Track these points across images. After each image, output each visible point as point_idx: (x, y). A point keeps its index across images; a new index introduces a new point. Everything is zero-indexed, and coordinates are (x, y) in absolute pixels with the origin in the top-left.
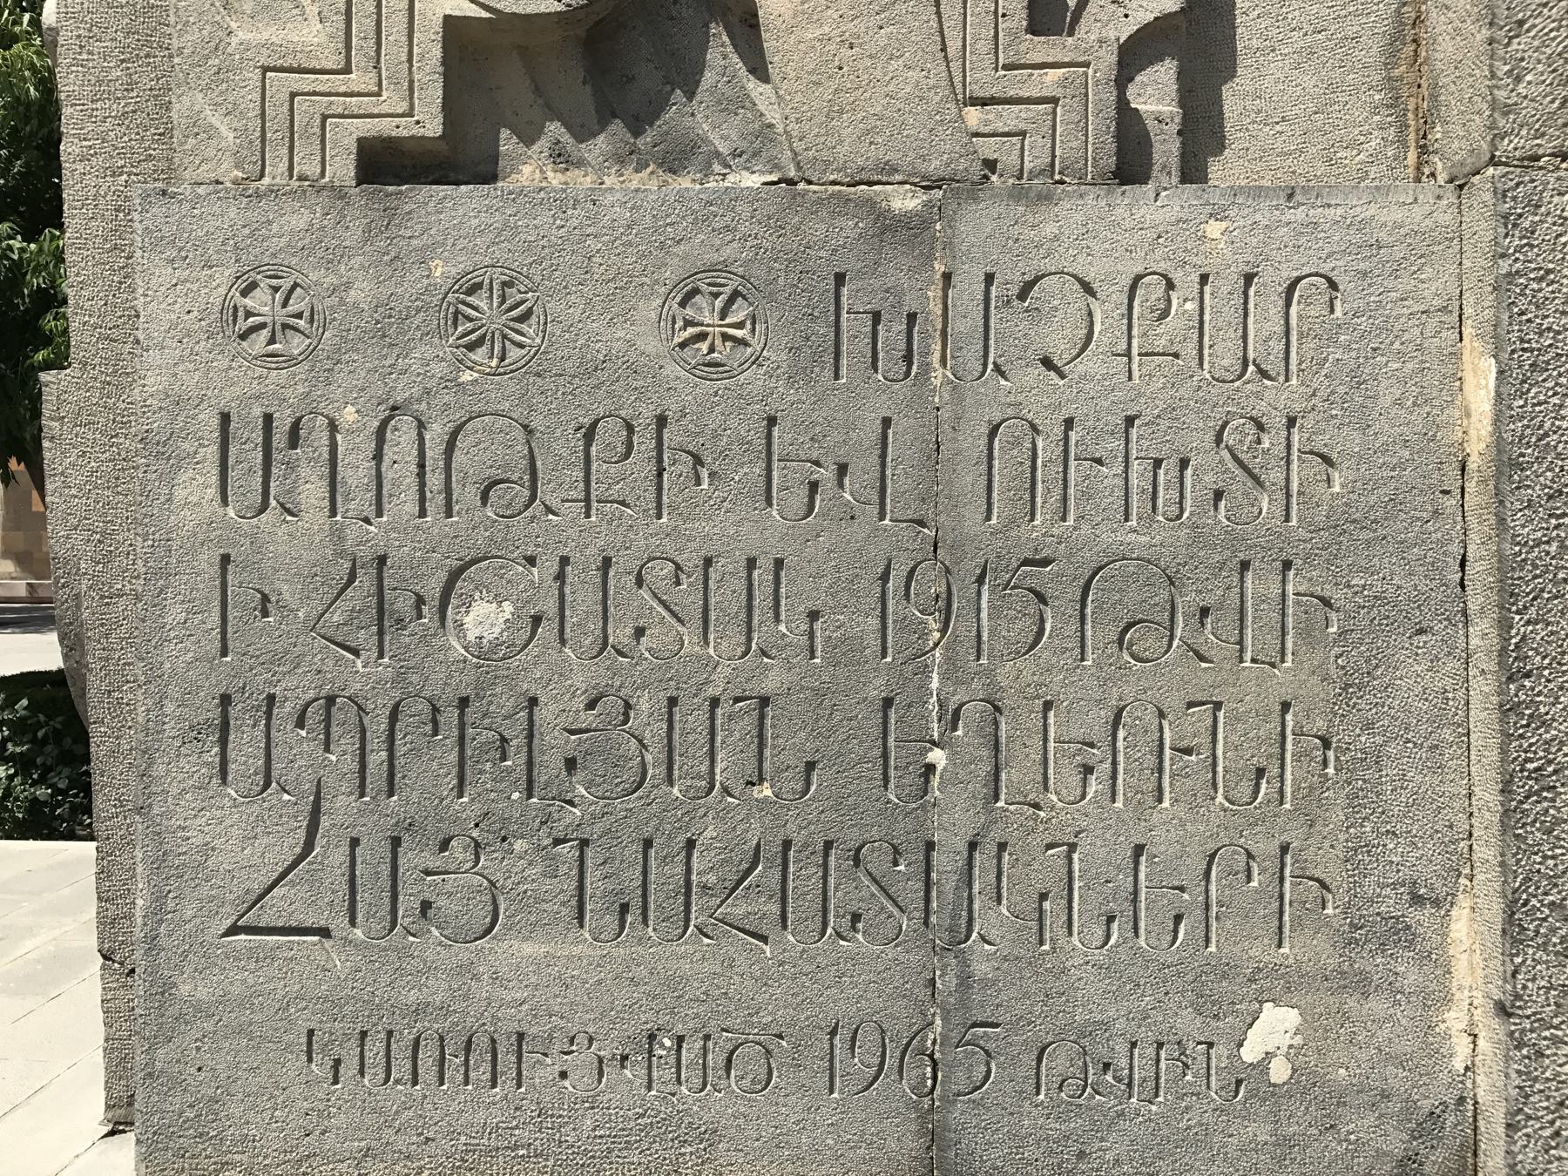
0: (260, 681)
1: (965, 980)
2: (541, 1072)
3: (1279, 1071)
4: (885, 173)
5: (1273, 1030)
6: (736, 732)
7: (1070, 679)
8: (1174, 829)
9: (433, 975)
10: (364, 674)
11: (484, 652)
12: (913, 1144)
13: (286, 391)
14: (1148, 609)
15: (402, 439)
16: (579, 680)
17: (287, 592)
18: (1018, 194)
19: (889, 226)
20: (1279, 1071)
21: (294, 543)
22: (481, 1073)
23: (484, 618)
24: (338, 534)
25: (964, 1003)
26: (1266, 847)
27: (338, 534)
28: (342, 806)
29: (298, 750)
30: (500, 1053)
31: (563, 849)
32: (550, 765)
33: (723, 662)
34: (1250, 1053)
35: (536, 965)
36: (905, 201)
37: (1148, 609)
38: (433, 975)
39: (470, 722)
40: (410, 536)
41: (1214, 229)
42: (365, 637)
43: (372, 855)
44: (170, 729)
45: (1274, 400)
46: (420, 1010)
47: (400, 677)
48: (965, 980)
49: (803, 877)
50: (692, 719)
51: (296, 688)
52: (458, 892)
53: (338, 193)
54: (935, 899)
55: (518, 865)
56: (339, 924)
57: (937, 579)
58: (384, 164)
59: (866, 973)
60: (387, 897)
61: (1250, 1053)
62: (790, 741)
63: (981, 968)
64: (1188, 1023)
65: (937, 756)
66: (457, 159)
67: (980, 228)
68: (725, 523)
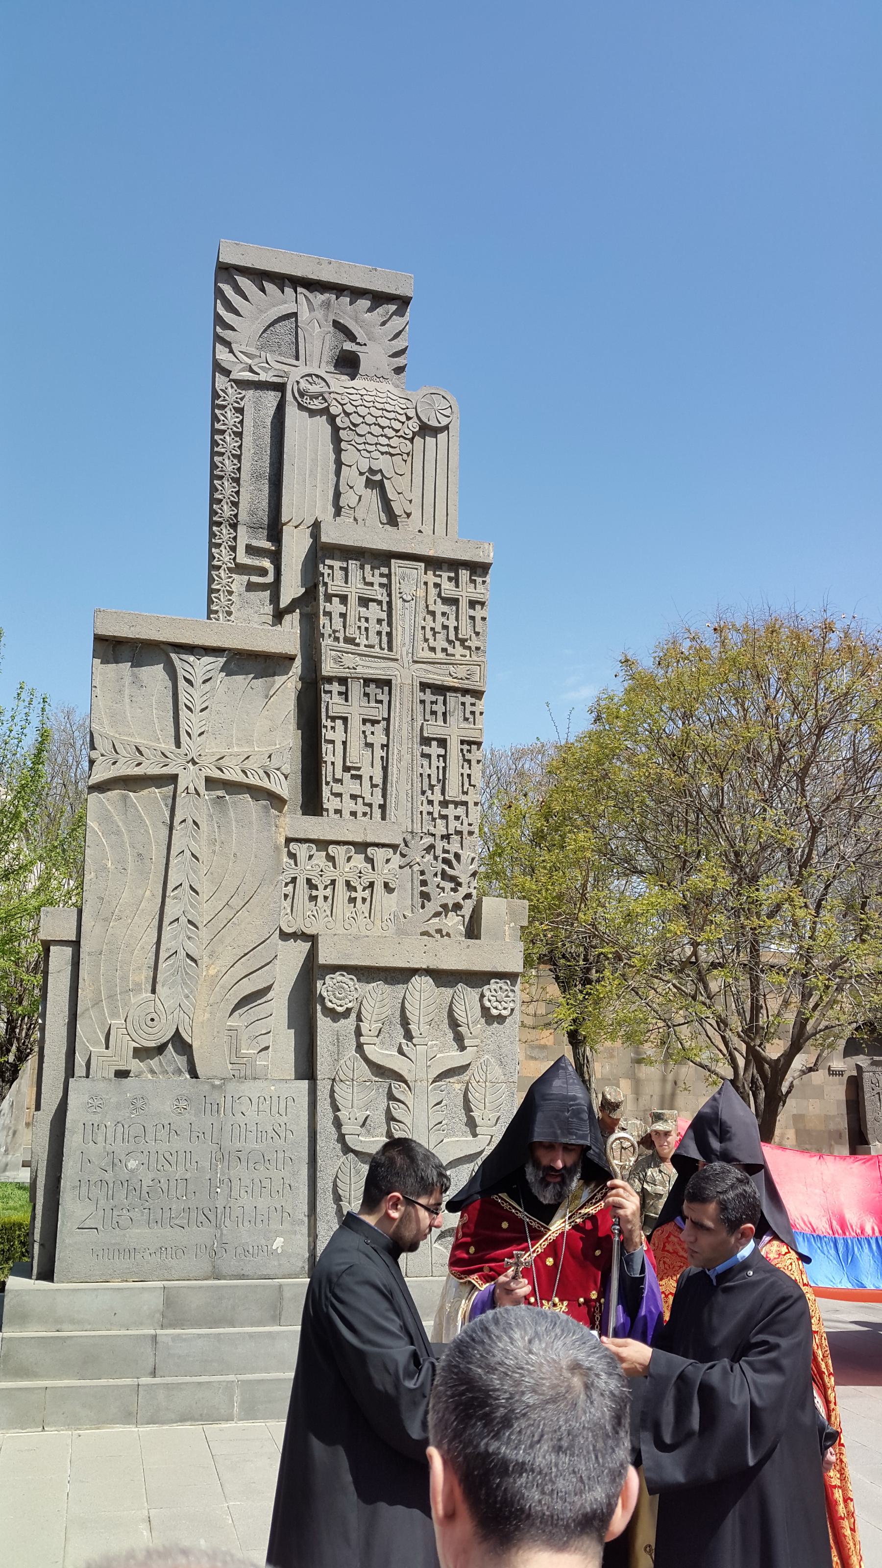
0: (86, 1178)
1: (222, 1234)
2: (139, 1256)
3: (279, 1251)
4: (215, 1077)
5: (279, 1242)
6: (182, 1184)
8: (262, 1203)
10: (109, 1176)
11: (132, 1171)
12: (210, 1268)
13: (96, 1119)
15: (120, 1129)
16: (151, 1175)
17: (93, 1159)
18: (238, 1081)
19: (214, 1086)
20: (279, 1251)
22: (127, 1256)
24: (105, 1147)
25: (221, 1239)
26: (279, 1207)
27: (105, 1147)
28: (102, 1202)
29: (95, 1192)
31: (146, 1211)
32: (144, 1193)
33: (180, 1173)
34: (274, 1247)
35: (139, 1235)
36: (217, 1082)
39: (128, 1184)
40: (120, 1147)
41: (273, 1088)
42: (109, 1169)
43: (108, 1212)
44: (68, 1187)
45: (285, 1119)
46: (115, 1244)
47: (115, 1176)
48: (222, 1234)
49: (193, 1214)
50: (173, 1183)
51: (94, 1178)
53: (110, 1080)
55: (136, 1214)
56: (100, 1227)
57: (221, 1155)
59: (204, 1234)
61: (274, 1247)
62: (191, 1187)
63: (225, 1232)
64: (263, 1242)
65: (218, 1190)
67: (231, 1087)
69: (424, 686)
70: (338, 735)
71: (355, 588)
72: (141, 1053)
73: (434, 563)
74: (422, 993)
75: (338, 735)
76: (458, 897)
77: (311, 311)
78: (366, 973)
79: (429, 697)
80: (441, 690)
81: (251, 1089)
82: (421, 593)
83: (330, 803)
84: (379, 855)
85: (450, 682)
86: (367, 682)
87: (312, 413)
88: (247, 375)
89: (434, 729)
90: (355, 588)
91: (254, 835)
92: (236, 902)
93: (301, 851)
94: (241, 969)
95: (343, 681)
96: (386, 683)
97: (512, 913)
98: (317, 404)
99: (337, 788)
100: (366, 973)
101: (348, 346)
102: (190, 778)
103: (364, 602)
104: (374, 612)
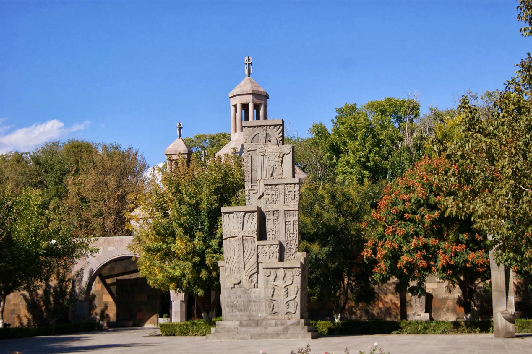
5: (260, 315)
7: (253, 304)
9: (234, 314)
14: (256, 301)
21: (229, 300)
23: (235, 302)
30: (236, 316)
35: (237, 313)
37: (256, 301)
38: (234, 314)
39: (235, 306)
52: (234, 310)
54: (249, 311)
59: (247, 313)
60: (232, 311)
66: (234, 288)
67: (250, 290)
68: (242, 299)
70: (269, 223)
71: (270, 193)
72: (234, 284)
75: (269, 223)
76: (293, 252)
79: (286, 212)
81: (254, 290)
82: (284, 191)
85: (290, 209)
88: (250, 149)
89: (287, 219)
90: (270, 193)
92: (249, 258)
94: (250, 269)
97: (303, 255)
98: (262, 154)
99: (269, 233)
104: (274, 196)
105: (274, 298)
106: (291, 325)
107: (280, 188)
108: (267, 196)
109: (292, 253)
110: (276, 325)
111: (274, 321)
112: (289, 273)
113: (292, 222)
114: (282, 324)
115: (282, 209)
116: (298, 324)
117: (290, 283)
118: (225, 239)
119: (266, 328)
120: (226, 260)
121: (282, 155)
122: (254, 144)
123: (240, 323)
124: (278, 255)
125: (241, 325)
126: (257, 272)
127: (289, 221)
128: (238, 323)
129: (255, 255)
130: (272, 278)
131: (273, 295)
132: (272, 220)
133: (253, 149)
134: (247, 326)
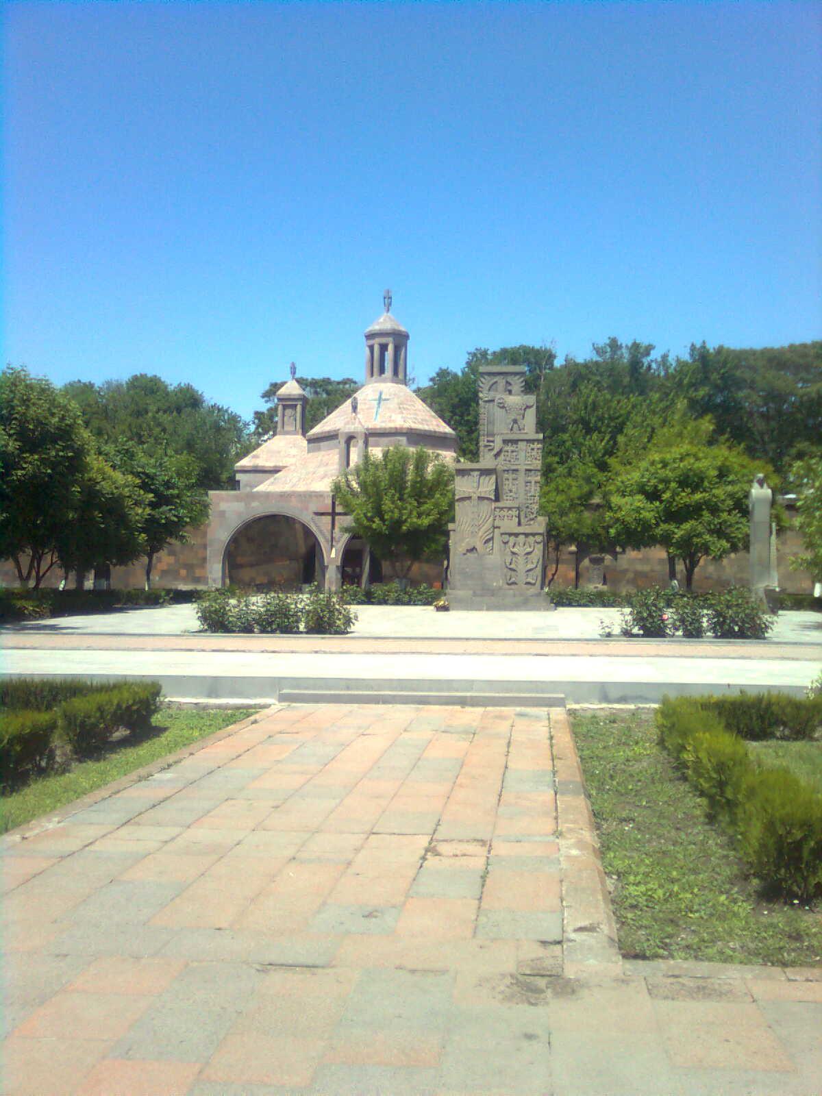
35: (469, 582)
58: (465, 554)
66: (465, 554)
69: (526, 470)
73: (528, 441)
74: (522, 538)
77: (501, 381)
78: (510, 534)
80: (530, 470)
81: (488, 556)
83: (505, 498)
84: (514, 510)
85: (532, 468)
86: (514, 470)
87: (501, 408)
91: (486, 507)
93: (498, 510)
95: (508, 471)
96: (517, 470)
98: (501, 405)
100: (510, 534)
101: (509, 388)
102: (475, 496)
103: (512, 452)
104: (514, 454)
105: (512, 566)
106: (532, 596)
107: (522, 445)
108: (506, 454)
109: (532, 516)
110: (514, 596)
111: (511, 592)
112: (531, 539)
113: (533, 483)
114: (521, 595)
115: (523, 468)
116: (538, 595)
117: (531, 550)
118: (458, 500)
119: (503, 600)
120: (457, 522)
121: (525, 406)
122: (492, 394)
123: (474, 592)
124: (517, 519)
125: (475, 594)
126: (492, 539)
127: (530, 482)
128: (471, 592)
129: (491, 519)
130: (511, 544)
131: (511, 564)
132: (511, 481)
133: (490, 398)
134: (482, 596)
